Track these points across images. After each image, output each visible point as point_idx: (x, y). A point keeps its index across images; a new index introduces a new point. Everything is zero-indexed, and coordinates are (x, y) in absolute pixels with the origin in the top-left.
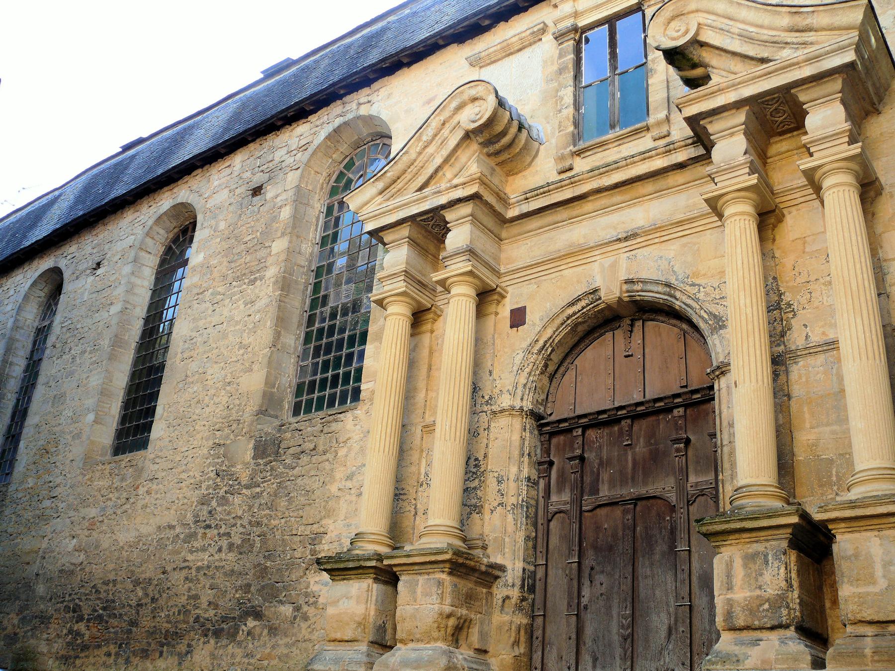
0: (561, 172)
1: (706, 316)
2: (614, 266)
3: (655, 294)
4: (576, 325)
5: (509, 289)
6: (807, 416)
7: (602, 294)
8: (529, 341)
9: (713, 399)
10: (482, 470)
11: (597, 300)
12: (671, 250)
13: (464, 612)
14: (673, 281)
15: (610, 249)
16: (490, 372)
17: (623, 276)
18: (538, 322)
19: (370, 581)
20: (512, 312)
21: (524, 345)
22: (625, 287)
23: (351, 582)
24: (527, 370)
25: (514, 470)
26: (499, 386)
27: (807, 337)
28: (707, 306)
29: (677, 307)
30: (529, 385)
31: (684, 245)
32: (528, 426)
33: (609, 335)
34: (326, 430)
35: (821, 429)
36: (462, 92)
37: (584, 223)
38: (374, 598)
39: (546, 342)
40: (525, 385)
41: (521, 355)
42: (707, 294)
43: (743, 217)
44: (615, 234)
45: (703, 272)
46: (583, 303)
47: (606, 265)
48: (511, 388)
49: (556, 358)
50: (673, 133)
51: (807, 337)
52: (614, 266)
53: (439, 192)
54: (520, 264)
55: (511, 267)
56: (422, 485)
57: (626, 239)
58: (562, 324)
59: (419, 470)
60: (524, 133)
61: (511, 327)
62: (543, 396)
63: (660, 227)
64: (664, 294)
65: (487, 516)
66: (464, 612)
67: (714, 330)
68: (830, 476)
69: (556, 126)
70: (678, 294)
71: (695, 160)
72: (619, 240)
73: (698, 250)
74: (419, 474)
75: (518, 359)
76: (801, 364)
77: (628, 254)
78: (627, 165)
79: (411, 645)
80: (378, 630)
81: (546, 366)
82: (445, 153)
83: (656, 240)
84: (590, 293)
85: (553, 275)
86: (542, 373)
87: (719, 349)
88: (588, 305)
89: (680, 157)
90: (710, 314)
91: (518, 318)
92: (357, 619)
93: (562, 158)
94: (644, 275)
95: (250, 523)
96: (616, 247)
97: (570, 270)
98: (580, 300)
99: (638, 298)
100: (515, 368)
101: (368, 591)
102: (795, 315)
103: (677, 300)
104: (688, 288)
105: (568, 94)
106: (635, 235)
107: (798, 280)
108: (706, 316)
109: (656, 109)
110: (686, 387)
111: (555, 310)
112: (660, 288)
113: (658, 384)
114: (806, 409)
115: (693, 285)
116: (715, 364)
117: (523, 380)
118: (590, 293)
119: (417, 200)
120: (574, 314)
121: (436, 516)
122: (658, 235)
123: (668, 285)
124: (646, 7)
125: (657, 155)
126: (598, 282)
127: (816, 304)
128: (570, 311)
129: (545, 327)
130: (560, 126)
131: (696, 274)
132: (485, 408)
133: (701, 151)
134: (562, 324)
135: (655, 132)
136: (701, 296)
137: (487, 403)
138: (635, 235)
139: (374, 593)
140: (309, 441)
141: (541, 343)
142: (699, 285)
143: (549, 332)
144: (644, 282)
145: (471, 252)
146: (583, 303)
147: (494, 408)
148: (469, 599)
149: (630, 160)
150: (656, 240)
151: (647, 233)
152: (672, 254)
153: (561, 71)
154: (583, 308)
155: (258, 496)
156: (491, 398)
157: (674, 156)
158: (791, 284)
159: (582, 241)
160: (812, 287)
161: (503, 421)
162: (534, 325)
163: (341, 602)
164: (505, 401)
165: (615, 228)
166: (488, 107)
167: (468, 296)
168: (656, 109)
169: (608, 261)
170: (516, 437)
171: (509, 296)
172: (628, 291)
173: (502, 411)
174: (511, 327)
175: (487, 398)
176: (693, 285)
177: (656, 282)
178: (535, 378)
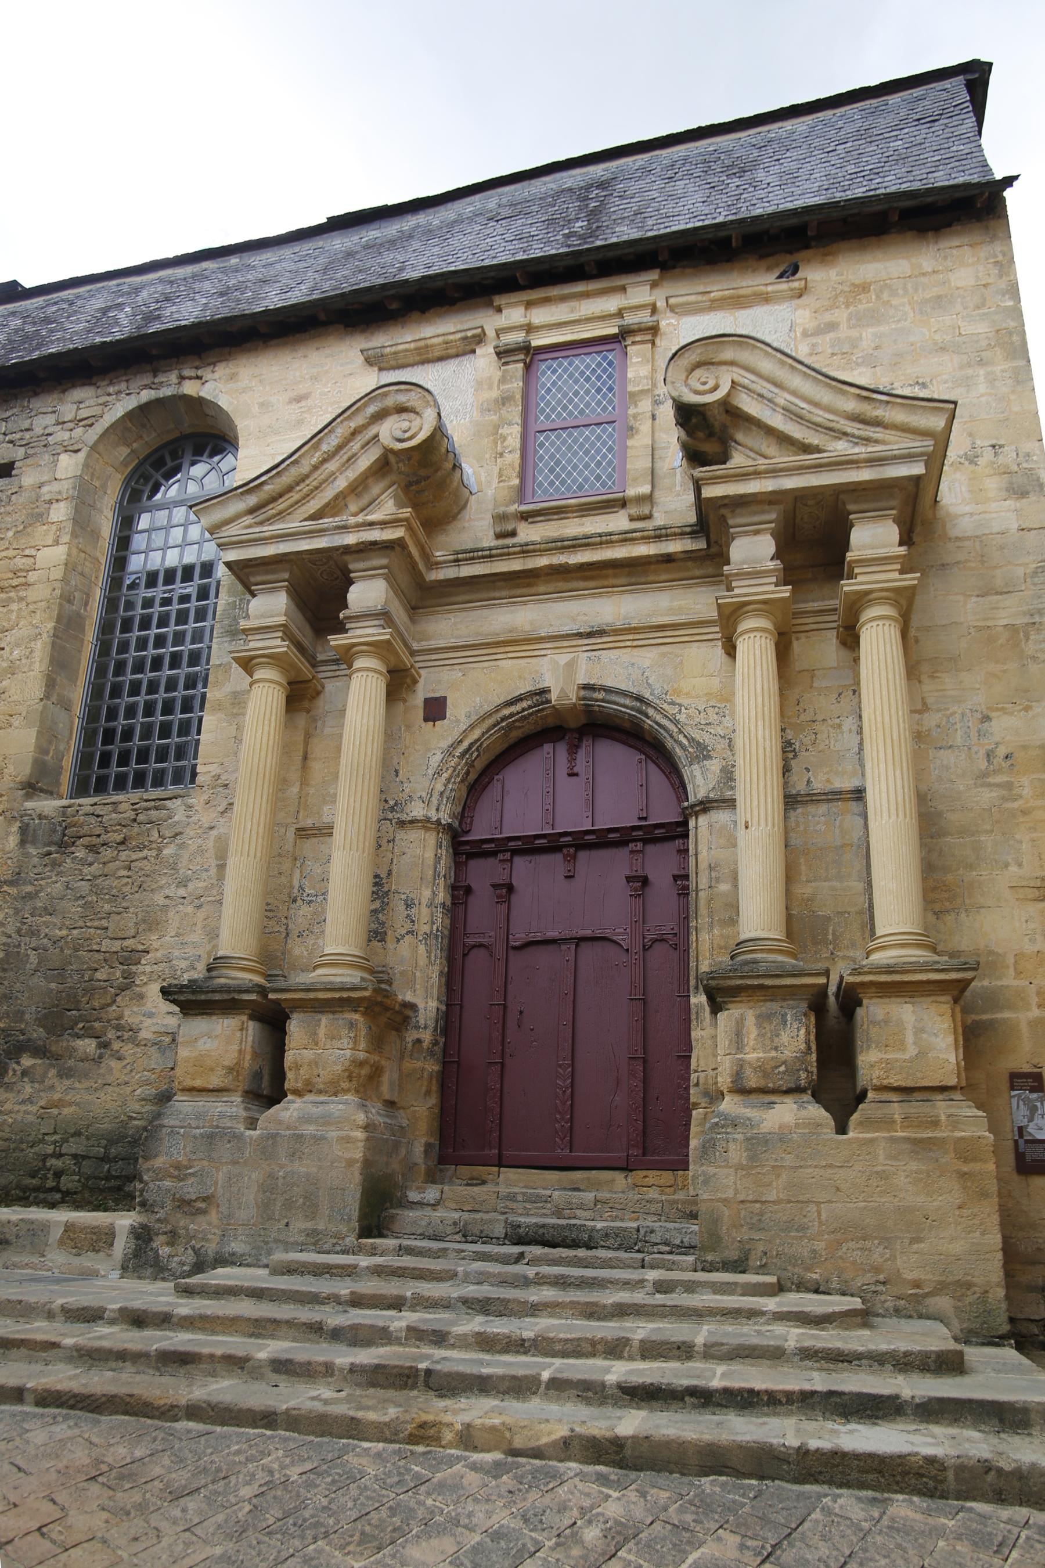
0: (499, 536)
1: (685, 741)
2: (571, 665)
3: (623, 707)
4: (510, 727)
5: (422, 671)
6: (803, 868)
7: (553, 696)
8: (450, 741)
9: (687, 836)
10: (386, 889)
11: (543, 703)
12: (646, 658)
13: (377, 1058)
14: (647, 695)
15: (565, 644)
16: (397, 772)
17: (582, 680)
18: (463, 719)
19: (245, 1018)
20: (427, 701)
21: (445, 744)
22: (582, 693)
23: (214, 1018)
24: (446, 775)
25: (427, 893)
26: (407, 790)
27: (809, 782)
28: (688, 730)
29: (646, 726)
30: (447, 793)
31: (664, 655)
32: (444, 843)
33: (548, 747)
34: (141, 818)
35: (817, 884)
36: (385, 395)
37: (531, 606)
38: (250, 1039)
39: (471, 745)
40: (442, 794)
41: (439, 757)
42: (689, 717)
43: (765, 635)
44: (575, 627)
45: (685, 691)
46: (524, 704)
47: (562, 663)
48: (424, 795)
49: (479, 765)
50: (656, 515)
51: (809, 782)
52: (571, 665)
53: (345, 527)
54: (442, 643)
55: (426, 644)
56: (295, 901)
57: (590, 635)
58: (495, 726)
59: (291, 882)
60: (458, 471)
61: (426, 720)
62: (459, 809)
63: (635, 628)
64: (632, 709)
65: (391, 945)
66: (377, 1058)
67: (693, 760)
68: (826, 935)
69: (496, 471)
70: (651, 712)
71: (689, 556)
72: (580, 635)
73: (681, 663)
74: (292, 887)
75: (436, 760)
76: (799, 810)
77: (589, 654)
78: (601, 543)
79: (310, 1097)
80: (254, 1077)
81: (467, 773)
82: (352, 474)
83: (628, 643)
84: (536, 694)
85: (486, 664)
86: (462, 781)
87: (699, 780)
88: (530, 707)
89: (674, 547)
90: (691, 740)
91: (435, 710)
92: (226, 1063)
93: (500, 518)
94: (609, 683)
95: (19, 932)
96: (574, 643)
97: (510, 662)
98: (521, 700)
99: (597, 709)
100: (431, 772)
101: (242, 1030)
102: (795, 756)
103: (648, 717)
104: (665, 706)
105: (513, 434)
106: (601, 633)
107: (803, 717)
108: (685, 741)
109: (635, 480)
110: (645, 819)
111: (487, 708)
112: (628, 702)
113: (616, 812)
114: (802, 860)
115: (673, 703)
116: (692, 799)
117: (439, 787)
118: (536, 694)
119: (310, 532)
120: (512, 715)
121: (334, 940)
122: (631, 637)
123: (639, 699)
124: (629, 342)
125: (643, 538)
126: (548, 681)
127: (822, 747)
128: (506, 712)
129: (472, 727)
130: (500, 475)
131: (678, 692)
132: (390, 816)
133: (701, 544)
134: (495, 726)
135: (634, 511)
136: (682, 718)
137: (392, 809)
138: (601, 633)
139: (250, 1032)
140: (114, 831)
141: (465, 744)
142: (680, 705)
143: (476, 734)
144: (608, 690)
145: (384, 616)
146: (524, 704)
147: (404, 817)
148: (377, 1042)
149: (605, 540)
150: (628, 643)
151: (617, 632)
152: (647, 663)
153: (505, 400)
154: (524, 710)
155: (30, 896)
156: (396, 804)
157: (664, 544)
158: (793, 720)
159: (527, 627)
160: (817, 727)
161: (414, 835)
162: (458, 721)
163: (201, 1042)
164: (417, 810)
165: (574, 620)
166: (422, 428)
167: (375, 671)
168: (635, 480)
169: (563, 659)
170: (429, 855)
171: (422, 681)
172: (584, 699)
173: (412, 822)
174: (426, 720)
175: (392, 803)
176: (673, 703)
177: (624, 694)
178: (455, 787)
